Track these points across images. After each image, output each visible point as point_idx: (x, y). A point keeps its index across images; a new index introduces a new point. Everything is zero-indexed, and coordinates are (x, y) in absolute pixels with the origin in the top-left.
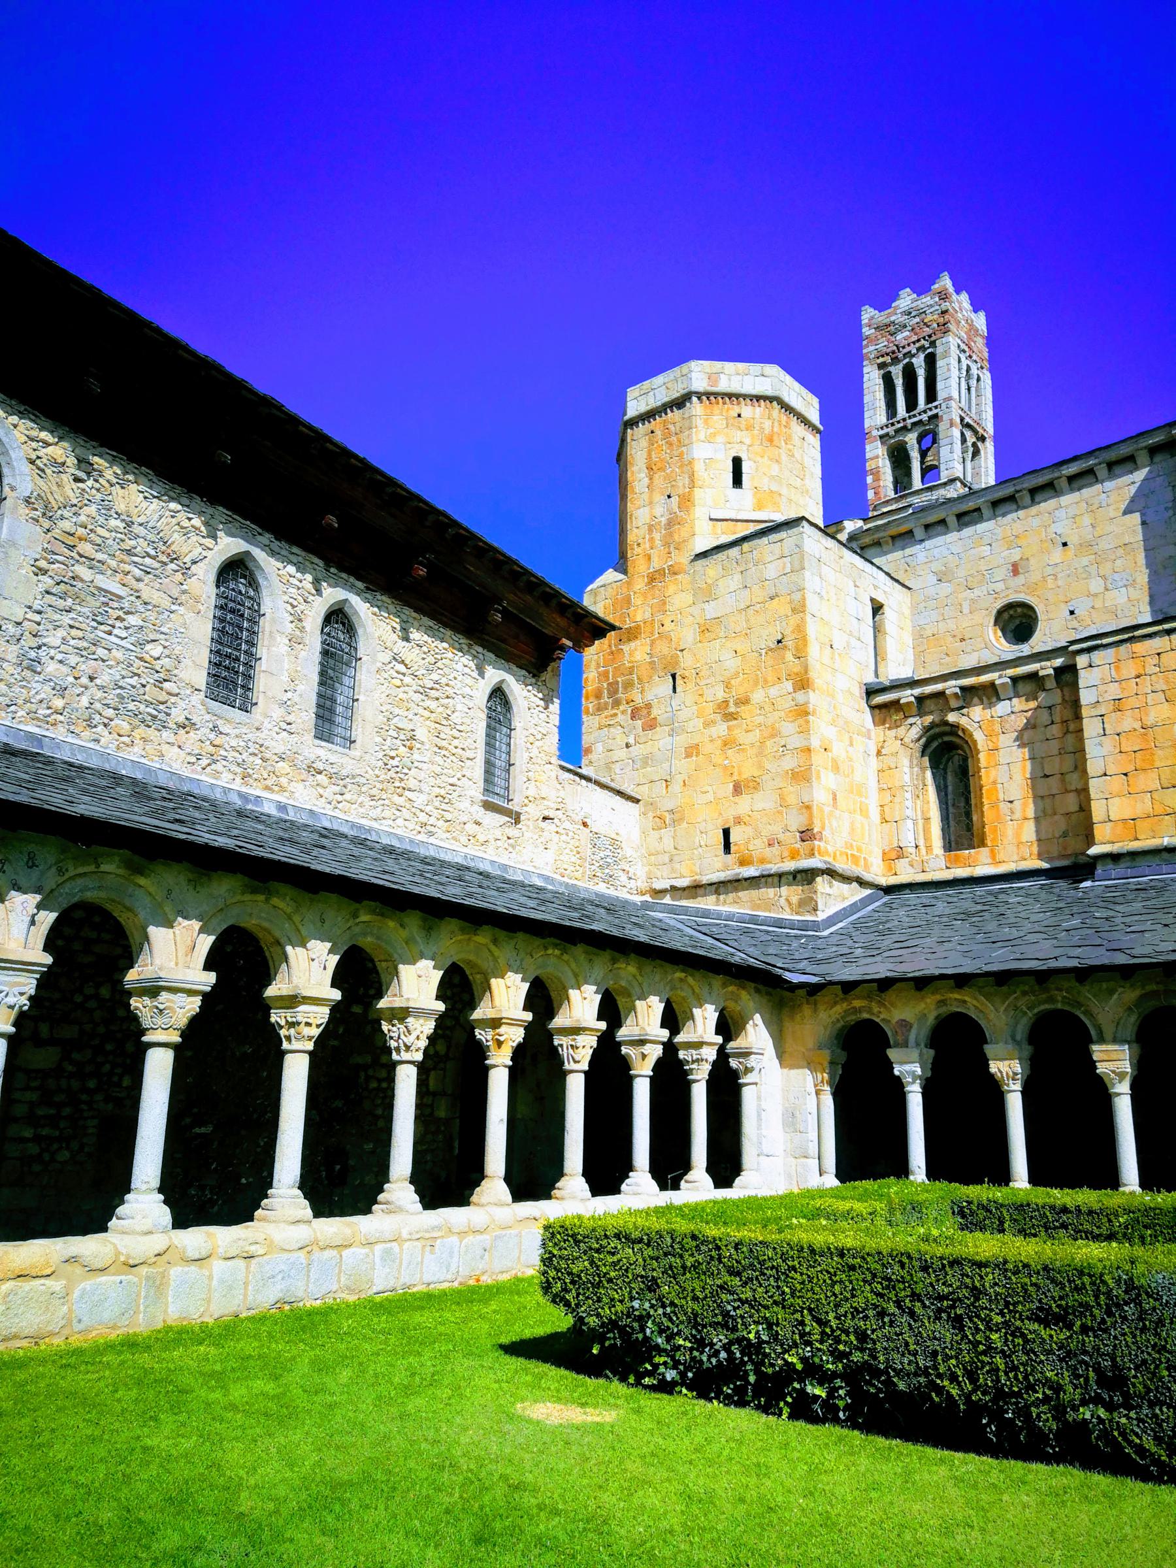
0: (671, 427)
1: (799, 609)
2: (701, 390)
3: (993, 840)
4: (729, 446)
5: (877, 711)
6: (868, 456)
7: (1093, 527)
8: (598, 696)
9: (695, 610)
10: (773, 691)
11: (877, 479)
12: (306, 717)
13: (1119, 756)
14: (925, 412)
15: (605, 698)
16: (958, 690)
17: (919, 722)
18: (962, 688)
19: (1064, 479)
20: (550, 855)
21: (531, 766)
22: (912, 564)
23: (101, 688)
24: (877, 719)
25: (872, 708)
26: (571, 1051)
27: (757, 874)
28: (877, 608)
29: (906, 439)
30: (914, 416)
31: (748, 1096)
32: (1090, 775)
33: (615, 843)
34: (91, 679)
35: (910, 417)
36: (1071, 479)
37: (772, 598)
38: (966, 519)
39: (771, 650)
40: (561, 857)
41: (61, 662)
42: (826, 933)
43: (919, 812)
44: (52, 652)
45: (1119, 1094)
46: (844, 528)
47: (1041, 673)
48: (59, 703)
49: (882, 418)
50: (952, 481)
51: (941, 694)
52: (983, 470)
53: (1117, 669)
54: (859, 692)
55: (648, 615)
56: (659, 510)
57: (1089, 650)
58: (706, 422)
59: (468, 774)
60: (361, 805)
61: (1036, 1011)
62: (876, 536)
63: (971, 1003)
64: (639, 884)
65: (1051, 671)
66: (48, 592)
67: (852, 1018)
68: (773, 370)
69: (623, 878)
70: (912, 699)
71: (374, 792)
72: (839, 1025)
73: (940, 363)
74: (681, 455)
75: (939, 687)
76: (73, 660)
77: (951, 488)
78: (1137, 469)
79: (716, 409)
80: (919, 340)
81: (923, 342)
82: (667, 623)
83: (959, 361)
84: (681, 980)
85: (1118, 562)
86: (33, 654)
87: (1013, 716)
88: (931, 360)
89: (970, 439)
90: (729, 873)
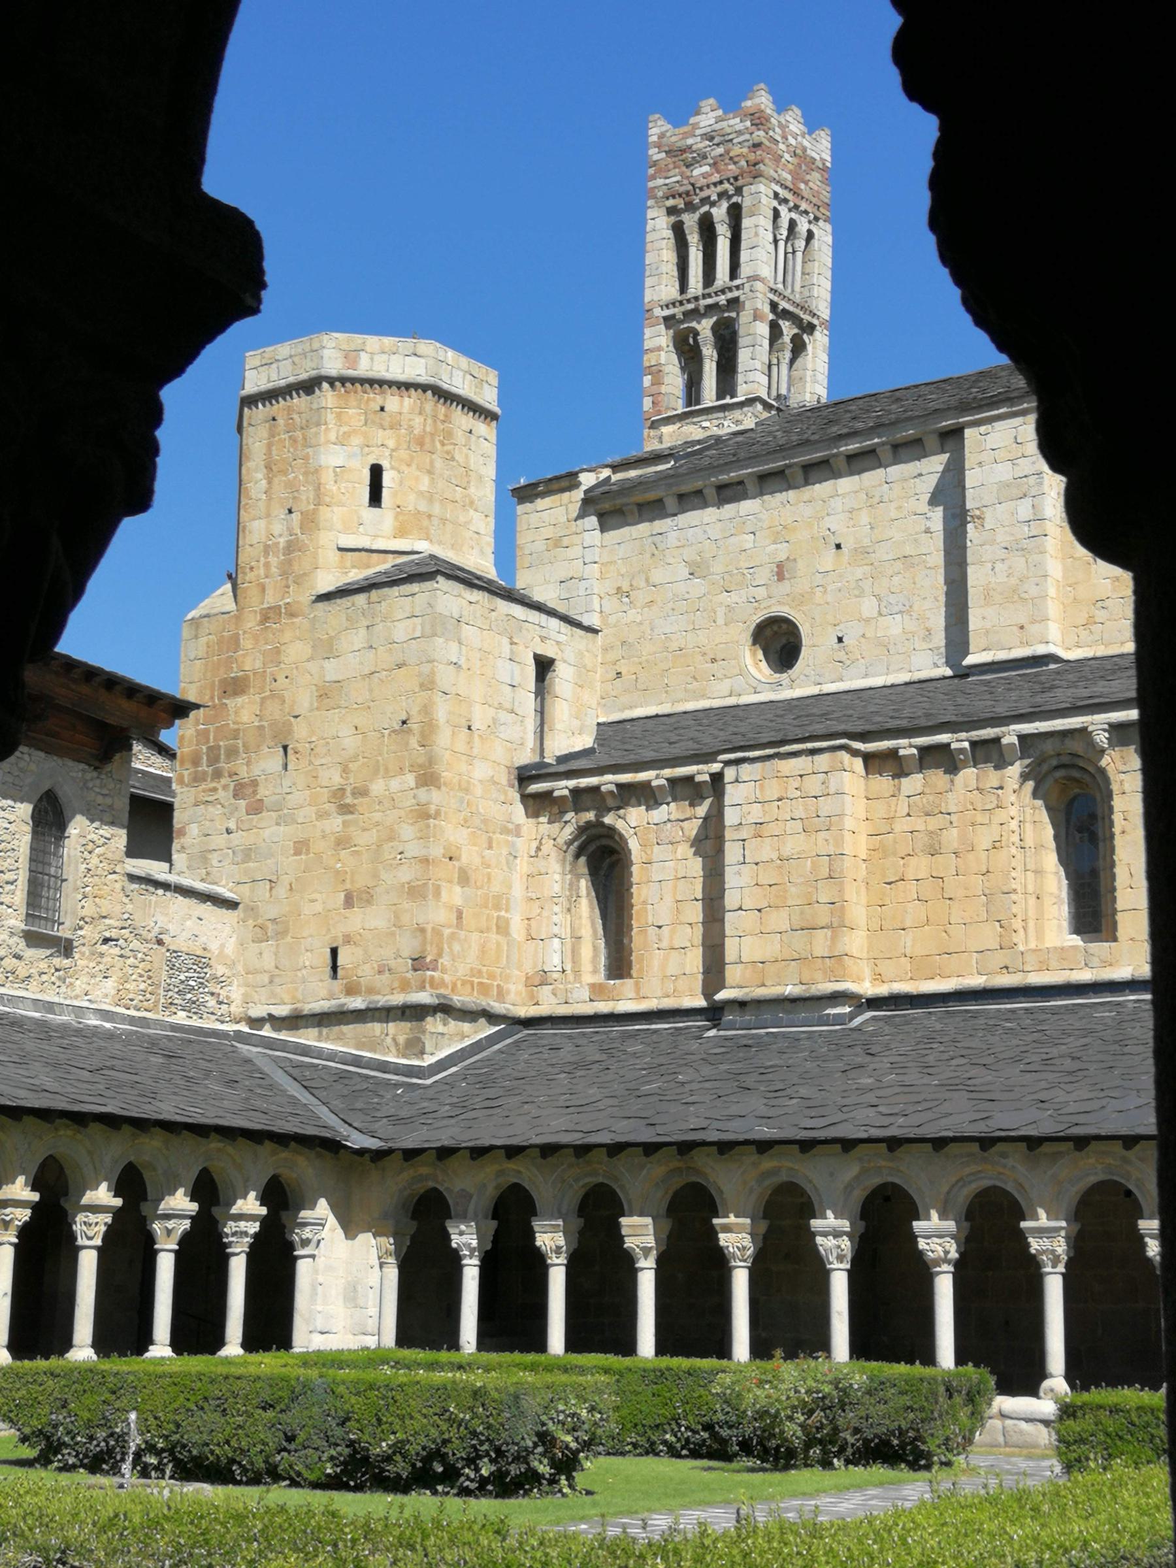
0: (295, 416)
1: (428, 685)
2: (333, 373)
3: (641, 970)
4: (366, 449)
5: (531, 802)
6: (647, 345)
7: (872, 528)
8: (196, 762)
9: (313, 667)
10: (395, 784)
11: (657, 382)
13: (757, 889)
14: (723, 292)
15: (204, 767)
16: (613, 788)
17: (573, 821)
18: (620, 786)
19: (842, 459)
20: (110, 985)
22: (661, 546)
24: (530, 811)
25: (525, 798)
26: (84, 1228)
28: (544, 666)
29: (698, 327)
30: (709, 296)
31: (303, 1269)
32: (727, 908)
33: (201, 962)
35: (704, 296)
36: (851, 458)
37: (399, 666)
38: (728, 493)
39: (394, 731)
40: (127, 986)
42: (429, 1082)
43: (568, 930)
45: (643, 1269)
46: (580, 484)
47: (698, 778)
49: (671, 290)
50: (750, 402)
51: (596, 789)
52: (809, 373)
53: (762, 787)
54: (504, 778)
55: (258, 664)
56: (277, 528)
57: (738, 762)
58: (339, 416)
61: (581, 1183)
62: (619, 502)
63: (527, 1174)
64: (233, 1008)
65: (707, 778)
67: (421, 1188)
68: (427, 347)
69: (212, 1002)
70: (566, 792)
72: (406, 1193)
73: (746, 223)
74: (306, 458)
75: (593, 781)
79: (352, 400)
80: (721, 182)
81: (726, 185)
82: (281, 679)
83: (776, 214)
84: (219, 1150)
85: (895, 579)
87: (669, 825)
88: (735, 213)
90: (334, 1002)
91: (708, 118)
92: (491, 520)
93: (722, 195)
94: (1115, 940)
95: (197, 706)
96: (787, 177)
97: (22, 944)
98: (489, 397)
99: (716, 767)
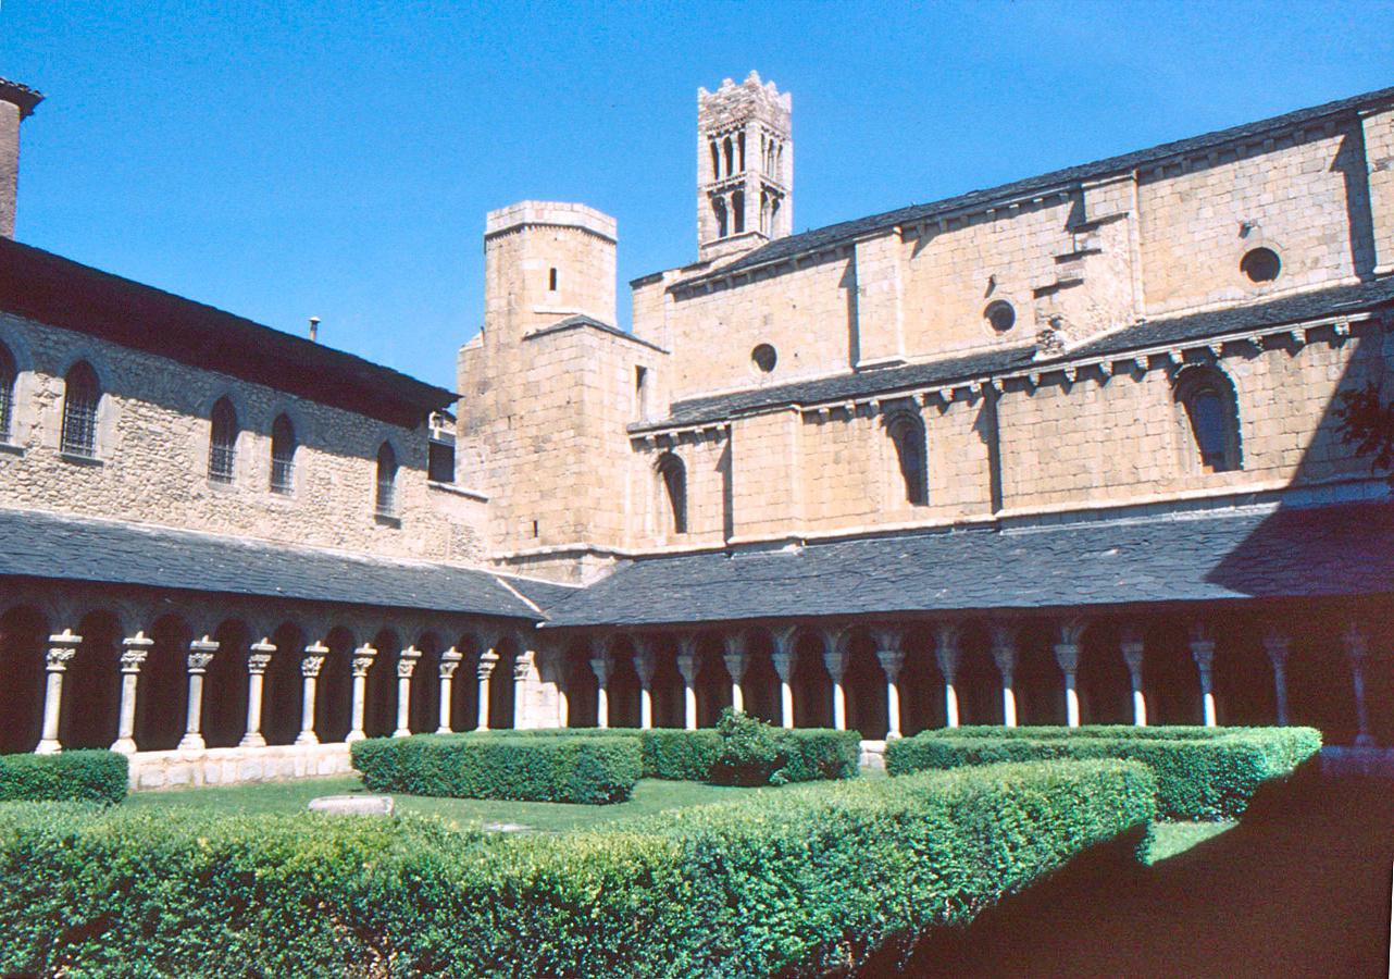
2: (530, 221)
6: (699, 206)
12: (265, 481)
21: (408, 488)
23: (153, 484)
27: (550, 551)
28: (641, 372)
33: (468, 530)
34: (148, 481)
35: (728, 180)
36: (800, 261)
38: (738, 281)
41: (133, 475)
44: (128, 470)
48: (132, 496)
49: (710, 178)
50: (751, 234)
51: (667, 435)
54: (621, 430)
59: (365, 499)
60: (298, 527)
66: (125, 439)
71: (305, 519)
73: (747, 142)
76: (139, 472)
77: (750, 239)
78: (838, 259)
85: (824, 323)
86: (119, 473)
89: (770, 198)
91: (728, 86)
92: (614, 296)
93: (736, 128)
94: (927, 505)
95: (461, 397)
96: (768, 118)
97: (374, 521)
98: (611, 233)
99: (727, 423)
